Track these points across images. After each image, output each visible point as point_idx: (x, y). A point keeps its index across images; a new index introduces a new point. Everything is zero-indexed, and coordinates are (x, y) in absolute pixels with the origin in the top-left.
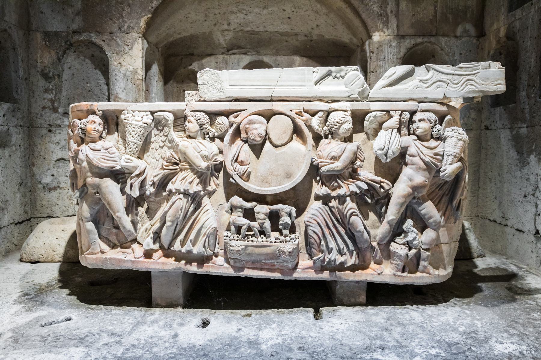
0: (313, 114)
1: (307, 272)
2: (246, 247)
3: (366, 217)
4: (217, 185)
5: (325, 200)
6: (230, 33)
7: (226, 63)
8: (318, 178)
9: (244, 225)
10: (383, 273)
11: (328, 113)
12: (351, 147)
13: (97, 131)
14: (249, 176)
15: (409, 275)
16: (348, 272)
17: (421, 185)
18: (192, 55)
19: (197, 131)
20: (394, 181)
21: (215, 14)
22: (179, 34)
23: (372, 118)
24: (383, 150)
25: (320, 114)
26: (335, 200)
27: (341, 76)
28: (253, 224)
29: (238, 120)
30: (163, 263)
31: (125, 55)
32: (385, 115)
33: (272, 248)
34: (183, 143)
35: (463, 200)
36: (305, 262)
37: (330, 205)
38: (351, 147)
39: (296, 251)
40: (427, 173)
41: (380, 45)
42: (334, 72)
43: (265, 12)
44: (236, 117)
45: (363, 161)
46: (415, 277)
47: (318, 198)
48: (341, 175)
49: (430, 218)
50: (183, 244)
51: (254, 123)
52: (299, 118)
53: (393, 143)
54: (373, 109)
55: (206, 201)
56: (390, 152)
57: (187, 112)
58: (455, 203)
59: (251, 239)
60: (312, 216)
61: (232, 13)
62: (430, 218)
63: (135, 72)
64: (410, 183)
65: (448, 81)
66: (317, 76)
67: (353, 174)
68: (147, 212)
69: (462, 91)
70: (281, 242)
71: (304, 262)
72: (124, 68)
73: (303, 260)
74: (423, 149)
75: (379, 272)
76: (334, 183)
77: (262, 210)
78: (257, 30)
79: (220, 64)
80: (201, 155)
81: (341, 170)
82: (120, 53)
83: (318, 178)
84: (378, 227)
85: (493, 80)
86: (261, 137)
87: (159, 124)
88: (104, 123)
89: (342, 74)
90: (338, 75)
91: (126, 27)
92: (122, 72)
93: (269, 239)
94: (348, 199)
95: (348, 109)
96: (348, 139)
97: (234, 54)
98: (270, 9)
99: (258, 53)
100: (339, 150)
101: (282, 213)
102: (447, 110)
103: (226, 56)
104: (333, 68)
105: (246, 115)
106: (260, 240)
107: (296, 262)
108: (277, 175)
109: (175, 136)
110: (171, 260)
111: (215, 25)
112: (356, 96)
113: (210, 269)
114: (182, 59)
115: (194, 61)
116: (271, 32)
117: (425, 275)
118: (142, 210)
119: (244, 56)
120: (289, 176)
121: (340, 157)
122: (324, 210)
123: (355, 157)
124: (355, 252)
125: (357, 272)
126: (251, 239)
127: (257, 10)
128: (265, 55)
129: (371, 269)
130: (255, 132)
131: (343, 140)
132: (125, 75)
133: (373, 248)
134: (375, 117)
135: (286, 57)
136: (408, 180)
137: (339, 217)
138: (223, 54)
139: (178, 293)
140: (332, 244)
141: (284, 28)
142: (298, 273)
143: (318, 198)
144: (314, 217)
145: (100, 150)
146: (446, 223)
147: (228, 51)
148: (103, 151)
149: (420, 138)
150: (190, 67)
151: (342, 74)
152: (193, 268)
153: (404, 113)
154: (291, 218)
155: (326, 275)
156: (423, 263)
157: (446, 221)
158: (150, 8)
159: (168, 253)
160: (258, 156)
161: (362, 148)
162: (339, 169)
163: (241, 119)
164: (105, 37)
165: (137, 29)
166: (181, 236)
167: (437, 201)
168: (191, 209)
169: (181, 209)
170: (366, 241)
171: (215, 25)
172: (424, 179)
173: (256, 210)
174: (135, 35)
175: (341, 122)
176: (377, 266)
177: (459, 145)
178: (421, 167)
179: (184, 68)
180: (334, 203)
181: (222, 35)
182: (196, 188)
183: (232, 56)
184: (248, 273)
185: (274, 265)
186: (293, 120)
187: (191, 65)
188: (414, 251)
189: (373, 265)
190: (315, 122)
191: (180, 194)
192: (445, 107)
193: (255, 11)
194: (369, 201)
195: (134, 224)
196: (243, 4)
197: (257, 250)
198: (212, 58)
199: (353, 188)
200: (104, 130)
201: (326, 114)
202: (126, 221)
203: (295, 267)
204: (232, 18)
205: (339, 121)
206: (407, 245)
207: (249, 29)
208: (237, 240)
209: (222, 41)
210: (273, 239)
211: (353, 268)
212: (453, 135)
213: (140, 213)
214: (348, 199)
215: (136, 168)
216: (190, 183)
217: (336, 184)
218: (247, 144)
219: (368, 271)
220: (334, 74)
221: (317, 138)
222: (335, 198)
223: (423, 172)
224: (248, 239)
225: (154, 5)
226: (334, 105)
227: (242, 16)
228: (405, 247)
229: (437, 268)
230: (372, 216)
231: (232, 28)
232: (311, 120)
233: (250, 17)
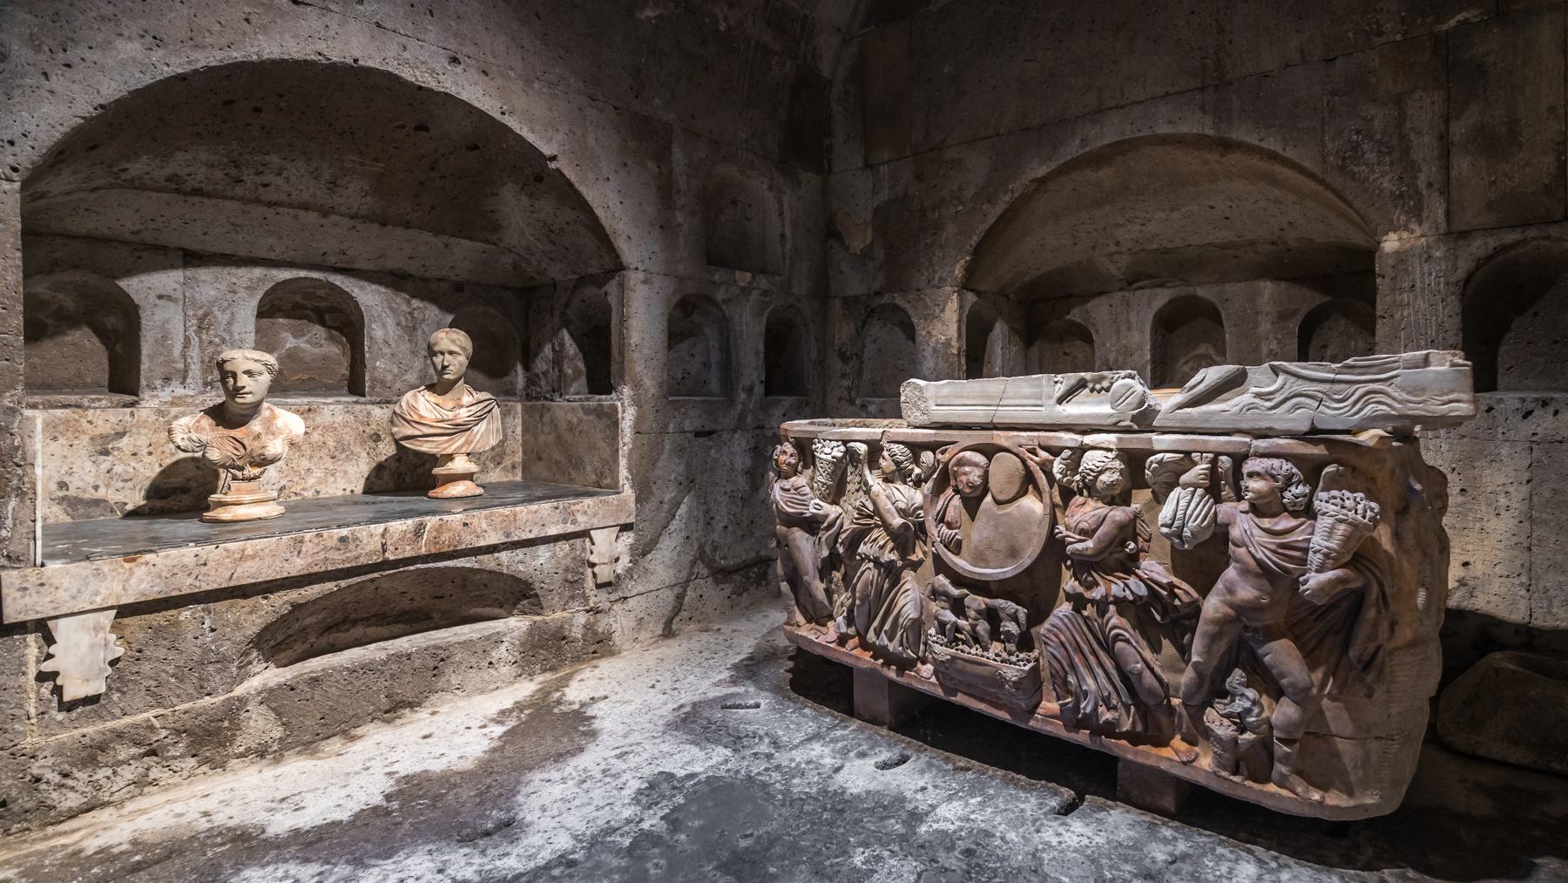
0: (1055, 452)
1: (1052, 723)
2: (954, 658)
3: (1156, 648)
4: (925, 553)
5: (1078, 602)
7: (1128, 304)
8: (1069, 563)
9: (948, 623)
10: (1194, 764)
11: (1082, 450)
12: (1119, 514)
13: (789, 464)
14: (959, 543)
15: (1248, 783)
16: (1124, 742)
17: (1250, 605)
18: (1070, 296)
19: (893, 472)
20: (1204, 591)
23: (1154, 465)
24: (1170, 526)
25: (1066, 453)
26: (1093, 606)
27: (1103, 389)
28: (962, 622)
29: (943, 458)
30: (857, 658)
31: (935, 321)
32: (1182, 459)
33: (989, 668)
35: (1391, 653)
37: (1085, 613)
38: (1119, 514)
40: (1265, 582)
41: (1401, 257)
42: (1091, 381)
43: (1176, 215)
44: (943, 453)
45: (1149, 541)
46: (1261, 791)
47: (1069, 597)
48: (1097, 563)
49: (1283, 676)
50: (878, 633)
51: (964, 465)
52: (1032, 460)
53: (1191, 516)
54: (1157, 447)
55: (908, 576)
56: (1187, 533)
57: (884, 443)
58: (1353, 653)
59: (961, 647)
60: (1051, 628)
61: (1118, 225)
62: (1283, 676)
63: (948, 344)
64: (1228, 597)
65: (1320, 395)
66: (1060, 389)
68: (843, 579)
69: (1356, 417)
70: (1002, 662)
71: (1049, 705)
72: (934, 339)
73: (1049, 701)
74: (1257, 532)
75: (1185, 759)
76: (1086, 578)
77: (976, 602)
78: (1170, 246)
80: (896, 508)
81: (1093, 556)
82: (930, 317)
83: (1069, 563)
84: (1181, 671)
85: (1436, 392)
86: (971, 487)
88: (799, 454)
89: (1105, 384)
90: (1098, 387)
91: (937, 278)
92: (931, 345)
93: (985, 653)
94: (1112, 608)
95: (1111, 447)
96: (1125, 500)
98: (1184, 210)
100: (1093, 519)
101: (1002, 615)
102: (1326, 453)
104: (1088, 375)
105: (956, 451)
106: (975, 651)
107: (1034, 701)
108: (998, 551)
110: (867, 656)
112: (1127, 423)
115: (1074, 307)
116: (1198, 246)
117: (1284, 792)
118: (837, 575)
119: (1159, 290)
120: (1014, 553)
121: (1094, 531)
122: (1074, 620)
123: (1128, 530)
124: (1132, 709)
125: (1141, 747)
126: (961, 647)
127: (1160, 214)
128: (1199, 284)
129: (1173, 748)
130: (964, 478)
131: (1109, 499)
132: (934, 349)
133: (1171, 710)
134: (1160, 462)
136: (1225, 591)
137: (1101, 638)
138: (1121, 289)
140: (1087, 684)
141: (1222, 236)
142: (1037, 720)
143: (1069, 597)
144: (1055, 630)
145: (789, 490)
146: (1340, 692)
147: (1130, 284)
148: (792, 491)
149: (1256, 510)
150: (1068, 317)
151: (1105, 384)
152: (892, 673)
153: (1220, 457)
154: (1019, 626)
155: (1083, 737)
156: (1280, 768)
157: (1342, 687)
160: (973, 516)
161: (1146, 517)
162: (1089, 552)
164: (911, 297)
166: (876, 624)
167: (1314, 642)
168: (886, 585)
169: (872, 582)
170: (1151, 692)
172: (1256, 593)
173: (967, 601)
174: (948, 289)
175: (1096, 470)
176: (1183, 746)
177: (1340, 532)
178: (1251, 568)
180: (1089, 611)
181: (1111, 261)
182: (889, 556)
183: (1138, 293)
184: (960, 699)
185: (998, 698)
186: (1023, 461)
187: (1068, 313)
188: (1248, 736)
189: (1177, 741)
190: (1057, 467)
191: (870, 561)
192: (1322, 446)
193: (1156, 216)
194: (1158, 618)
195: (829, 593)
196: (1132, 209)
197: (969, 667)
198: (1104, 299)
199: (1117, 589)
200: (799, 461)
201: (1077, 455)
203: (1032, 711)
204: (1119, 233)
205: (1093, 467)
206: (1238, 721)
207: (1155, 246)
208: (942, 645)
209: (1113, 269)
210: (991, 655)
211: (1134, 738)
212: (1326, 510)
213: (835, 580)
214: (1112, 608)
215: (826, 516)
216: (881, 547)
217: (1090, 579)
218: (958, 496)
219: (1166, 752)
220: (1091, 385)
221: (1067, 494)
222: (1093, 601)
223: (1255, 580)
224: (958, 645)
226: (1089, 439)
227: (1137, 227)
228: (1230, 723)
229: (1324, 787)
230: (1168, 647)
232: (1052, 462)
233: (1151, 228)
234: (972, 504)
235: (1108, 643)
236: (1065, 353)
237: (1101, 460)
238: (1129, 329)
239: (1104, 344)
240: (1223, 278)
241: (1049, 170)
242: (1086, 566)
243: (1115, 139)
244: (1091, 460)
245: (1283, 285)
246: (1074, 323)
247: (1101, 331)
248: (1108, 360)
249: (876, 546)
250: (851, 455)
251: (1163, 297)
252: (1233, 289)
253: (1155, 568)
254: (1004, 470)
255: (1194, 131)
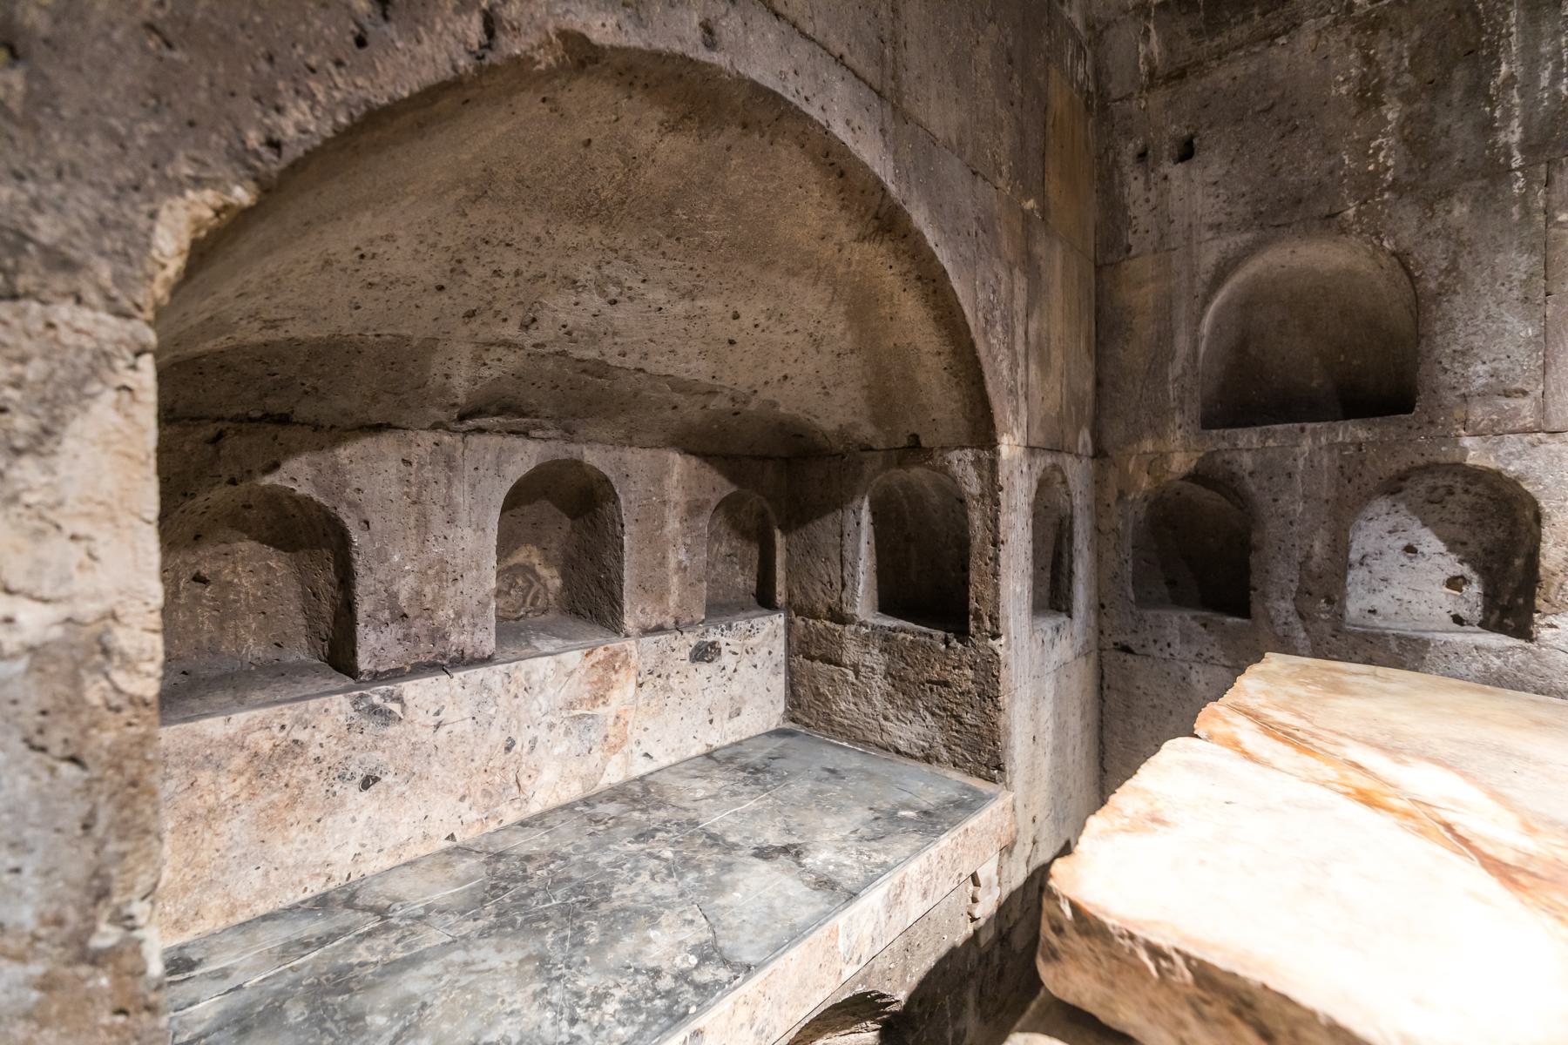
6: (512, 357)
7: (450, 463)
18: (284, 420)
21: (497, 273)
22: (273, 324)
78: (614, 361)
79: (421, 466)
97: (481, 431)
99: (569, 434)
103: (447, 438)
111: (471, 315)
114: (220, 436)
115: (290, 453)
119: (517, 442)
128: (588, 441)
135: (648, 452)
138: (434, 427)
141: (697, 368)
147: (462, 418)
150: (268, 480)
158: (254, 138)
165: (118, 279)
171: (471, 315)
179: (233, 482)
183: (474, 440)
187: (275, 466)
193: (650, 296)
196: (627, 259)
198: (386, 443)
207: (592, 354)
225: (287, 127)
231: (536, 336)
233: (621, 316)
236: (199, 579)
238: (450, 521)
239: (382, 556)
240: (628, 440)
241: (622, 41)
243: (770, 82)
245: (694, 461)
246: (276, 498)
247: (376, 525)
248: (393, 596)
251: (525, 457)
252: (636, 458)
255: (876, 170)
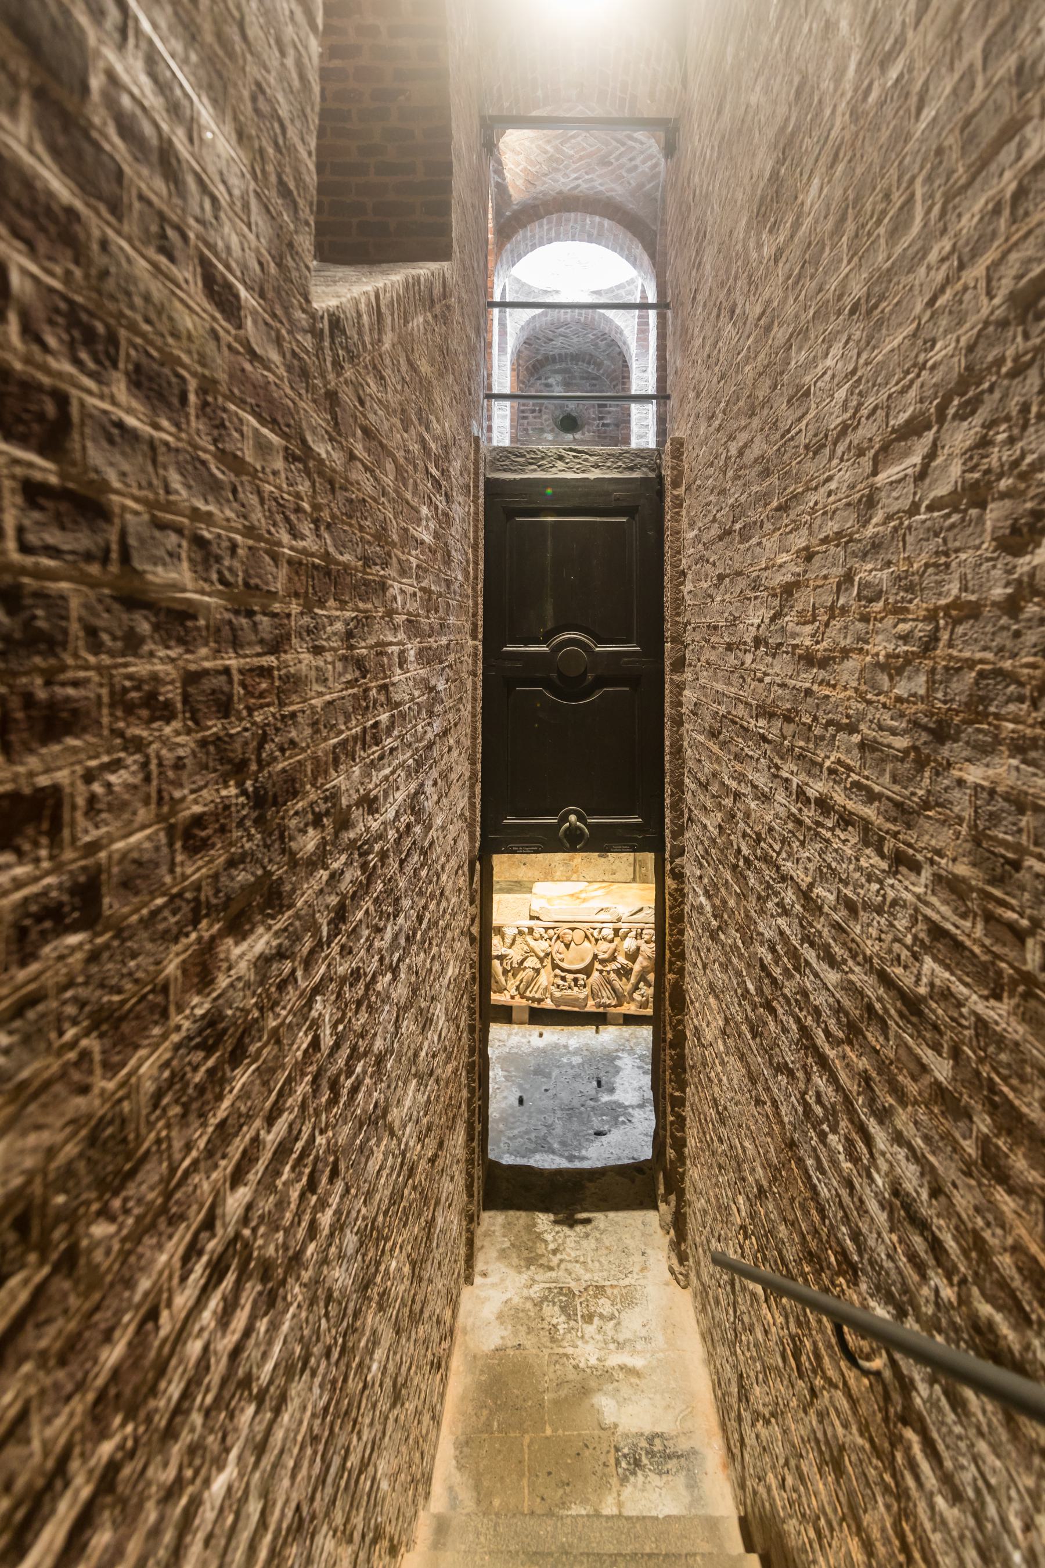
34: (532, 943)
36: (591, 1002)
38: (613, 946)
39: (586, 998)
67: (613, 958)
77: (570, 977)
87: (521, 933)
96: (612, 941)
109: (529, 938)
113: (543, 1005)
139: (526, 1016)
159: (522, 997)
163: (561, 932)
202: (502, 979)
234: (567, 946)
235: (609, 982)
237: (608, 932)
242: (603, 962)
244: (605, 932)
249: (532, 962)
250: (521, 933)
253: (622, 959)
254: (578, 935)
